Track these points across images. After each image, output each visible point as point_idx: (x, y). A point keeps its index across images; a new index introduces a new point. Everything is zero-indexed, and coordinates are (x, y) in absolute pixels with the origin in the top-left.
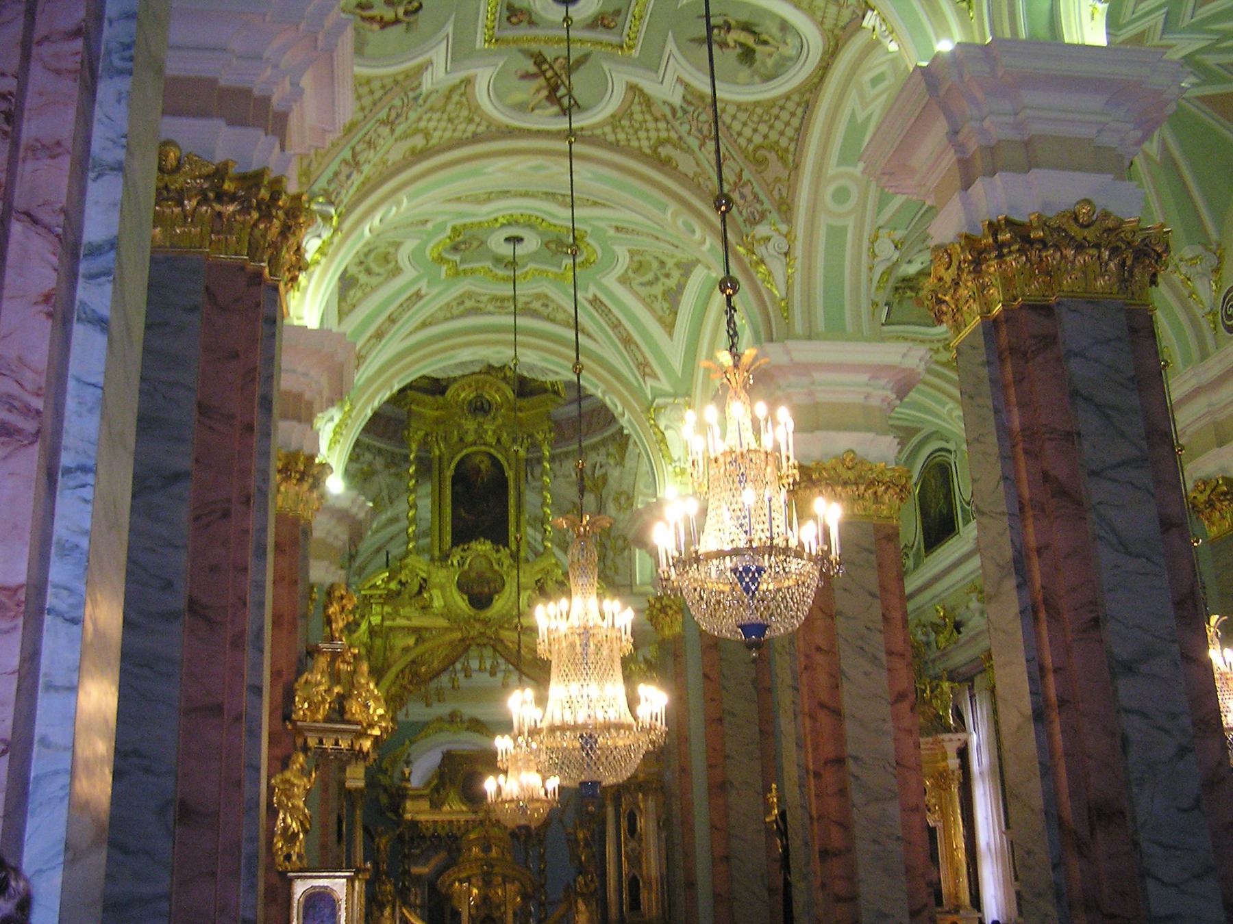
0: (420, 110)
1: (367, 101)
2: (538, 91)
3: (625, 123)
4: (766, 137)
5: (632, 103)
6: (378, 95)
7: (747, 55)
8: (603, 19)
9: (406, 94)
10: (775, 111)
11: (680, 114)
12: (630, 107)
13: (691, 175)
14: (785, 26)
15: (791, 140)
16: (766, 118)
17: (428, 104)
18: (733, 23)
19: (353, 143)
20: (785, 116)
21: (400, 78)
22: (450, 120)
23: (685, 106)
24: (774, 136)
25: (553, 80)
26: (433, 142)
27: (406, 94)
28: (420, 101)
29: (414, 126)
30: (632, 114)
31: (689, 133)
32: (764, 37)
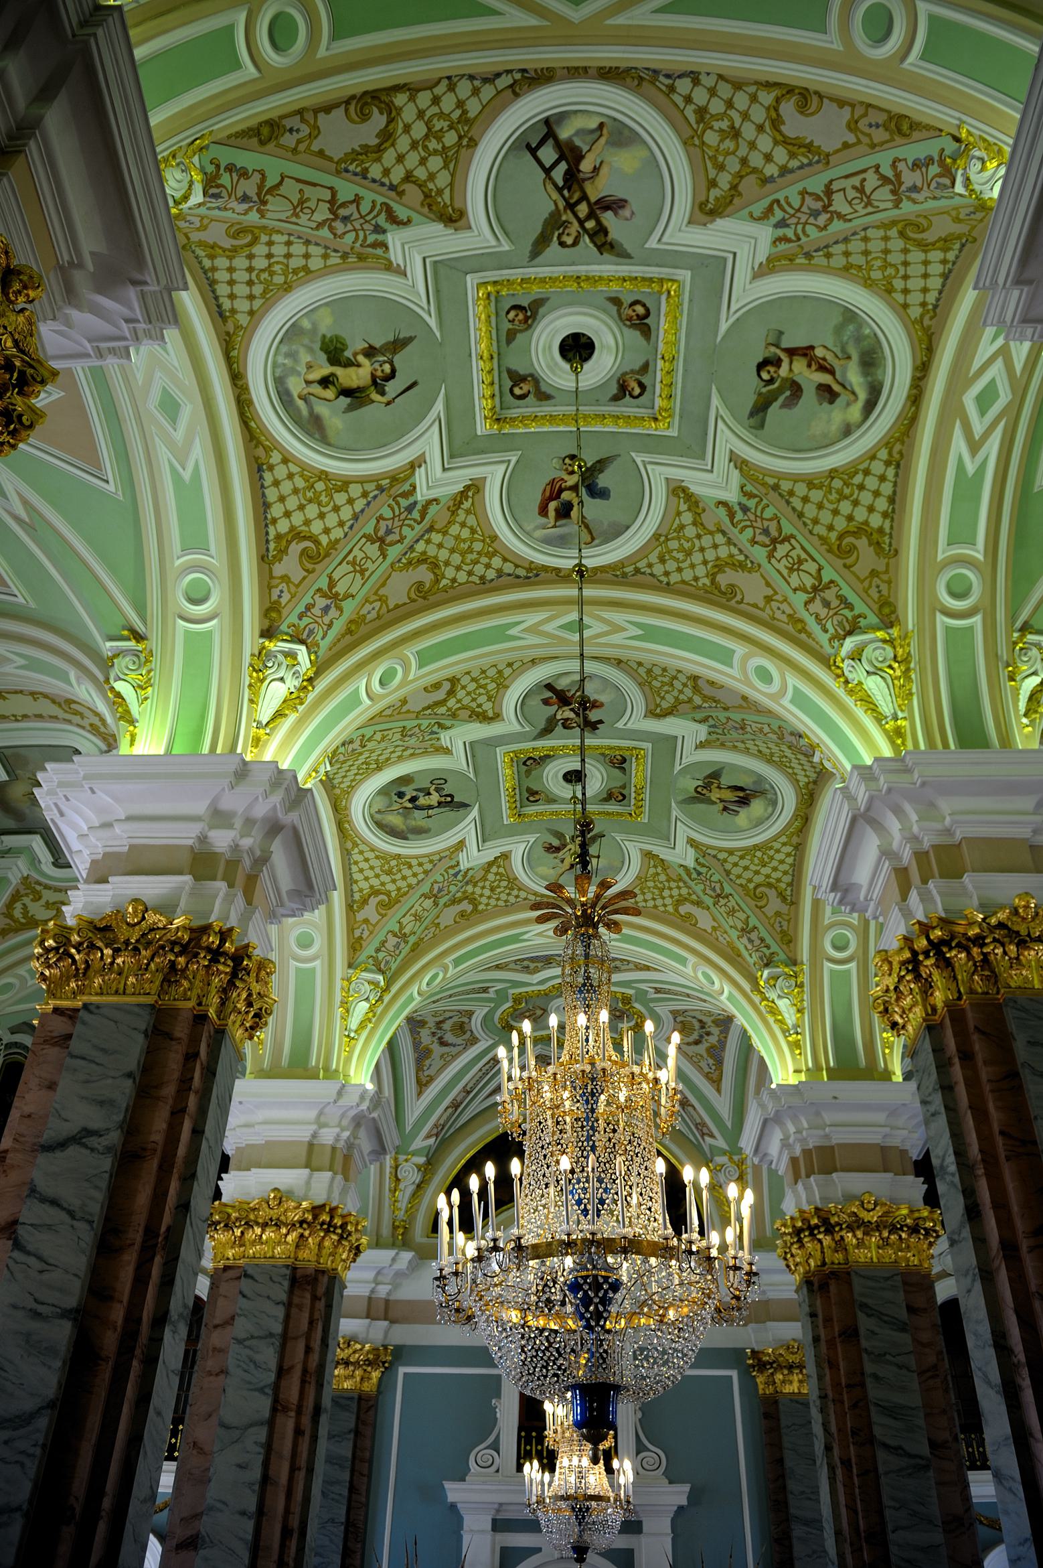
0: (780, 196)
1: (856, 246)
2: (596, 170)
3: (450, 138)
4: (251, 257)
5: (451, 184)
6: (838, 249)
7: (335, 353)
8: (526, 319)
9: (796, 234)
10: (258, 290)
11: (382, 220)
12: (452, 175)
13: (321, 116)
14: (314, 428)
15: (214, 269)
16: (265, 276)
17: (765, 203)
18: (375, 396)
19: (896, 212)
20: (241, 290)
21: (801, 260)
22: (735, 134)
23: (380, 237)
24: (241, 262)
25: (576, 196)
26: (767, 98)
27: (799, 239)
28: (778, 214)
29: (794, 164)
30: (446, 166)
31: (357, 200)
32: (330, 393)
